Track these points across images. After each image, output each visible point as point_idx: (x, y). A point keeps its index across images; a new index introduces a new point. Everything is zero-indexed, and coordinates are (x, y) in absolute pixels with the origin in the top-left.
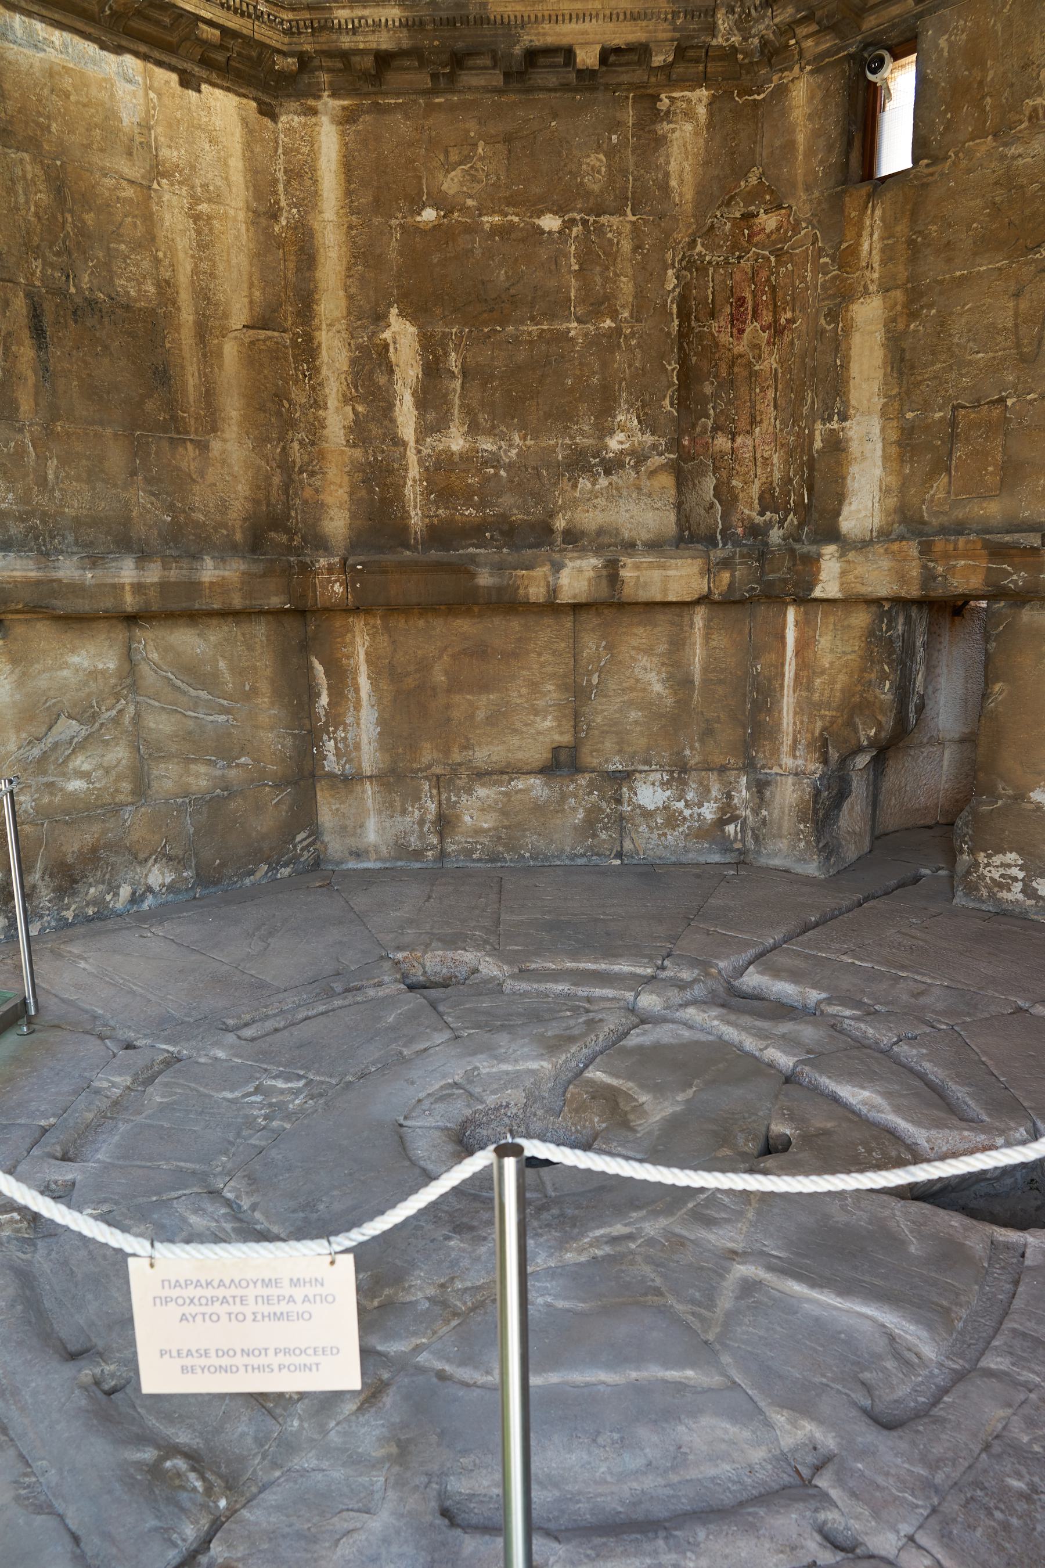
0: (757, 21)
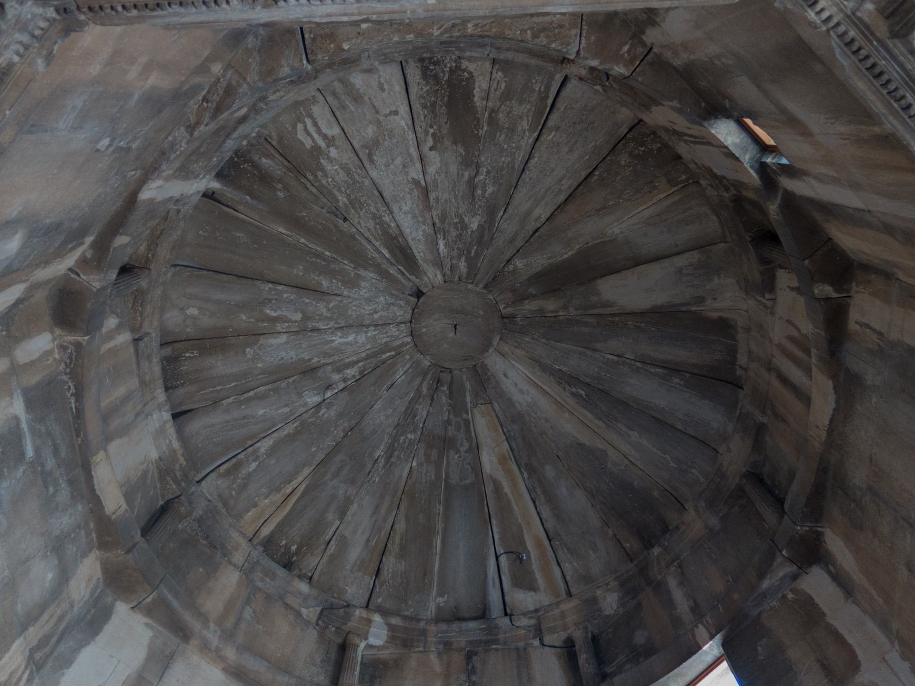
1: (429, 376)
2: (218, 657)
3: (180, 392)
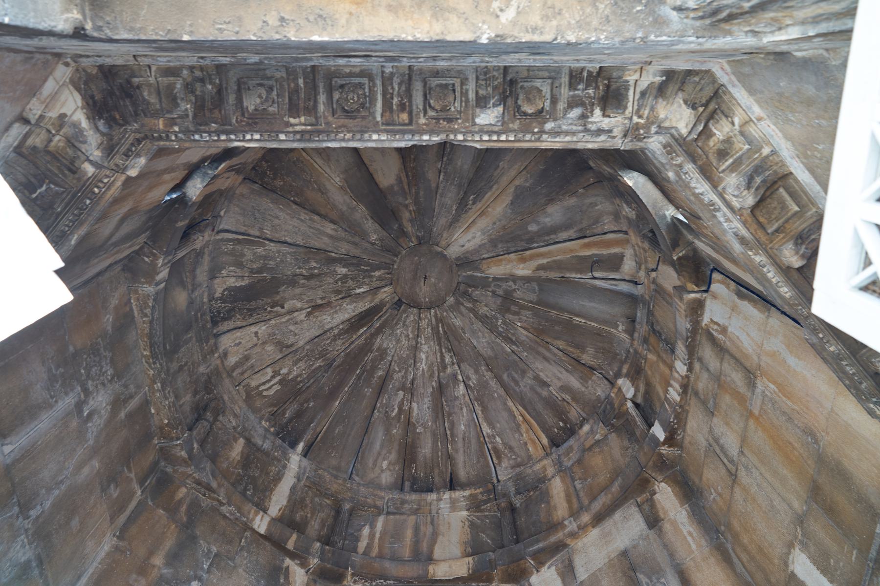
2: (583, 528)
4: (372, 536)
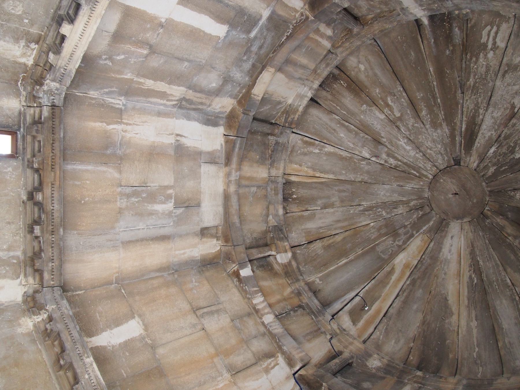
0: (49, 98)
1: (421, 201)
2: (228, 184)
3: (324, 93)
4: (322, 35)
